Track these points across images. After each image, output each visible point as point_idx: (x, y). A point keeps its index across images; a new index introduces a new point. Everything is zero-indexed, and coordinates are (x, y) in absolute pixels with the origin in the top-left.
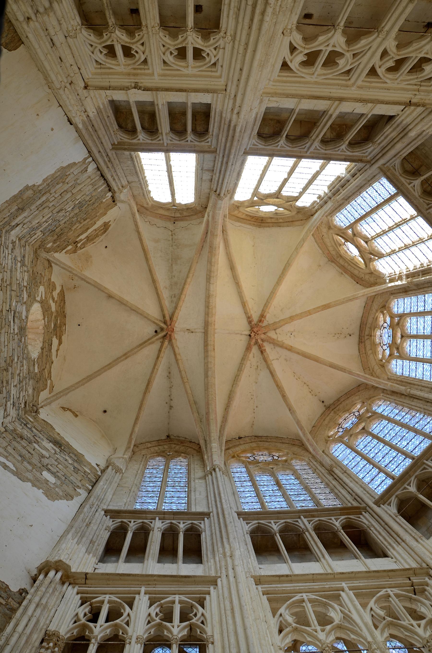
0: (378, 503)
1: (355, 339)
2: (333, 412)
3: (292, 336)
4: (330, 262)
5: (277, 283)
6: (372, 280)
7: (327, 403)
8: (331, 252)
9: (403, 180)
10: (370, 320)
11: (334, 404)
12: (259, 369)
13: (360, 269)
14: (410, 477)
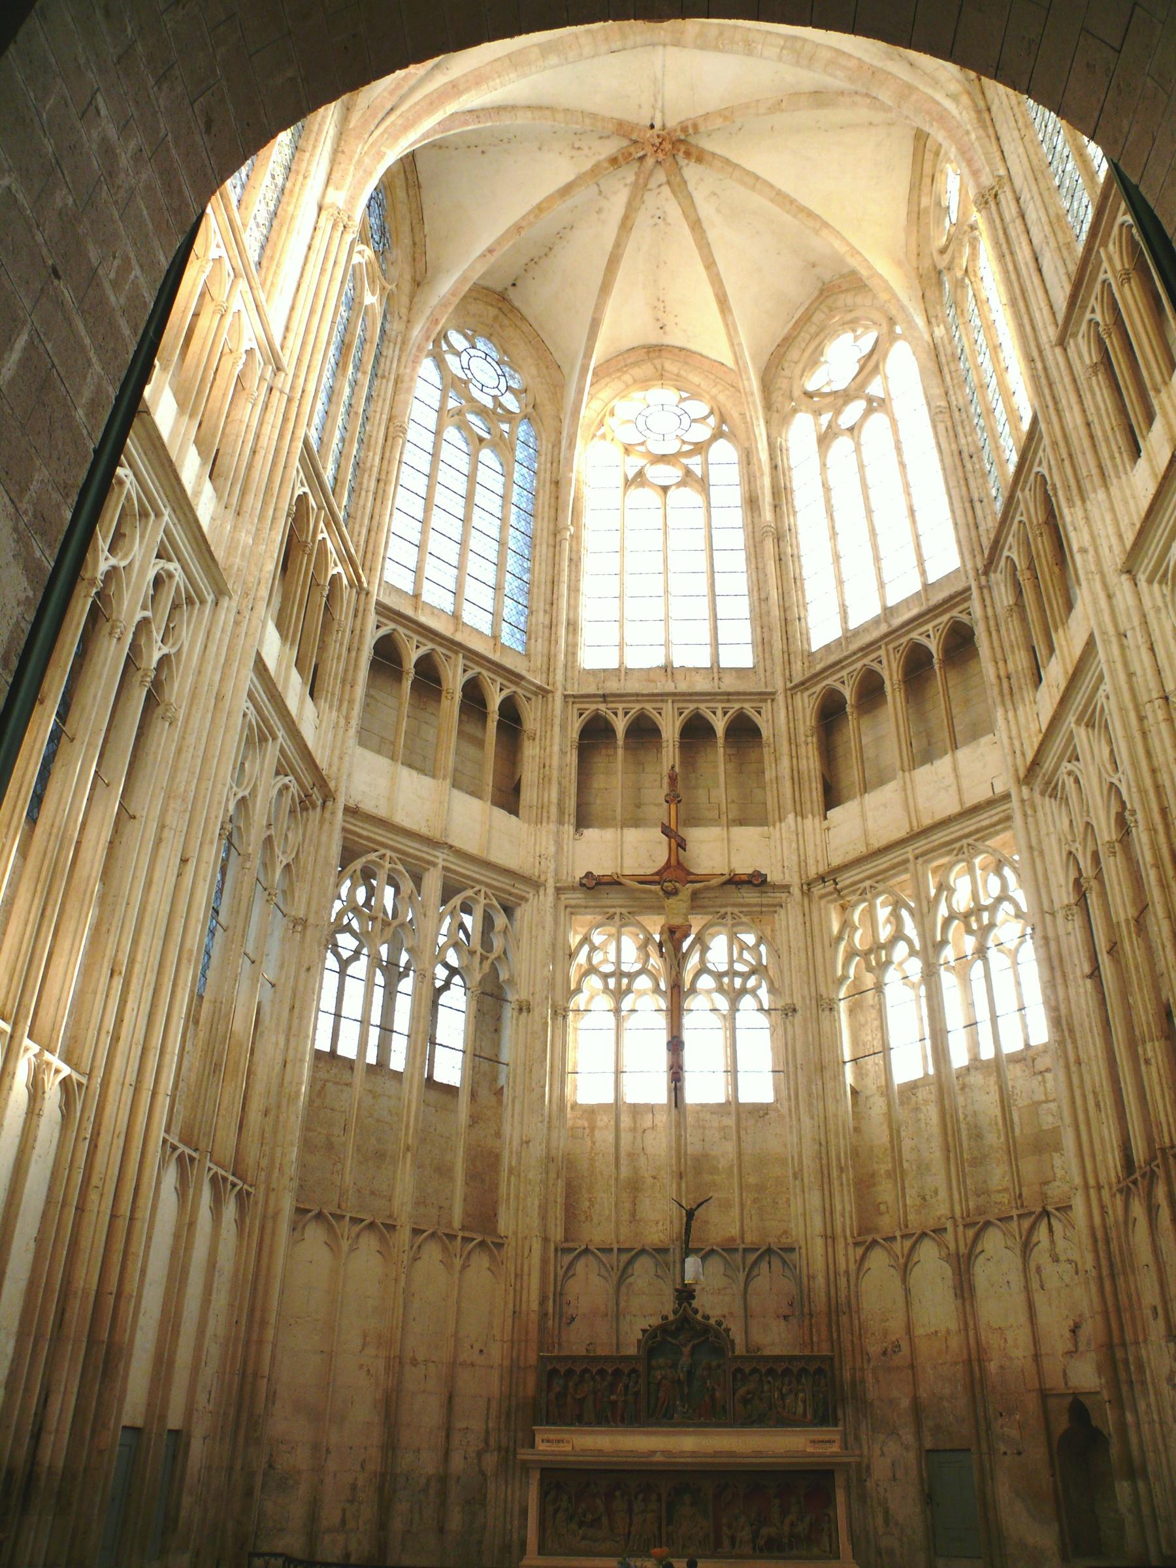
0: (378, 603)
1: (654, 338)
2: (496, 311)
3: (656, 220)
4: (819, 285)
5: (779, 193)
6: (777, 397)
7: (512, 294)
8: (842, 296)
9: (945, 618)
10: (696, 378)
11: (514, 309)
12: (575, 153)
13: (800, 366)
14: (432, 640)
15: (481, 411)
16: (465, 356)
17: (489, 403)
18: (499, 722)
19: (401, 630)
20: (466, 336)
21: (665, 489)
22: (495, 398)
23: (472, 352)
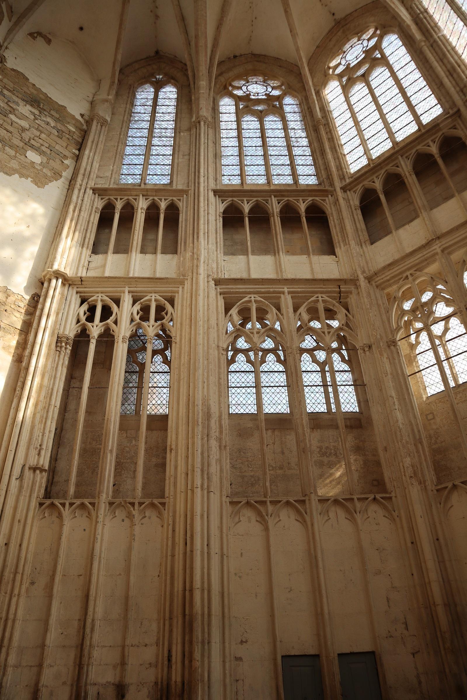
15: (258, 102)
16: (244, 88)
17: (264, 97)
18: (306, 217)
19: (235, 199)
20: (244, 80)
21: (363, 75)
22: (266, 95)
23: (247, 85)
